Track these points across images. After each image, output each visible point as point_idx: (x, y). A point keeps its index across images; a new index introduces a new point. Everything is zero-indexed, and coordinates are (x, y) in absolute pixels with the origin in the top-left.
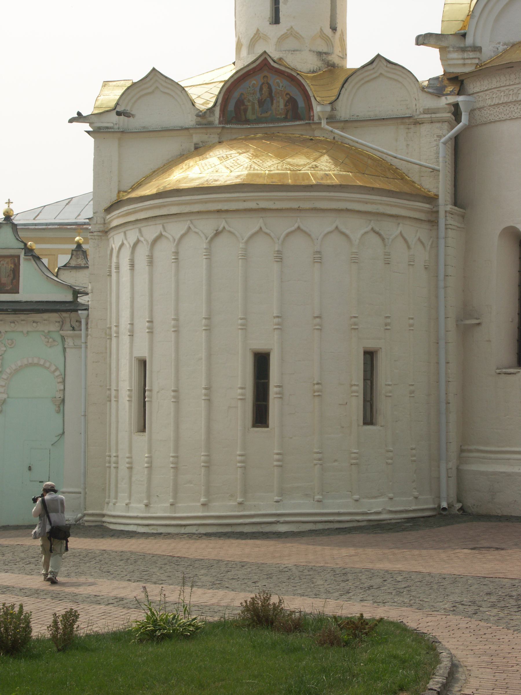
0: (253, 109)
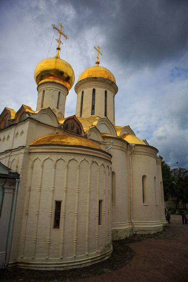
0: (70, 128)
